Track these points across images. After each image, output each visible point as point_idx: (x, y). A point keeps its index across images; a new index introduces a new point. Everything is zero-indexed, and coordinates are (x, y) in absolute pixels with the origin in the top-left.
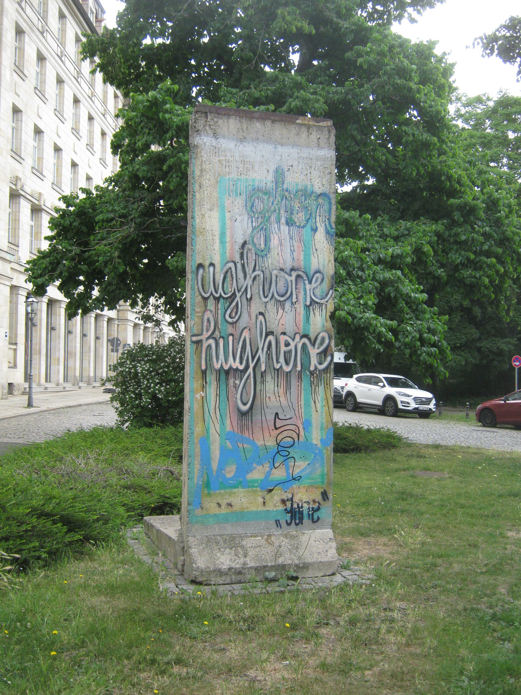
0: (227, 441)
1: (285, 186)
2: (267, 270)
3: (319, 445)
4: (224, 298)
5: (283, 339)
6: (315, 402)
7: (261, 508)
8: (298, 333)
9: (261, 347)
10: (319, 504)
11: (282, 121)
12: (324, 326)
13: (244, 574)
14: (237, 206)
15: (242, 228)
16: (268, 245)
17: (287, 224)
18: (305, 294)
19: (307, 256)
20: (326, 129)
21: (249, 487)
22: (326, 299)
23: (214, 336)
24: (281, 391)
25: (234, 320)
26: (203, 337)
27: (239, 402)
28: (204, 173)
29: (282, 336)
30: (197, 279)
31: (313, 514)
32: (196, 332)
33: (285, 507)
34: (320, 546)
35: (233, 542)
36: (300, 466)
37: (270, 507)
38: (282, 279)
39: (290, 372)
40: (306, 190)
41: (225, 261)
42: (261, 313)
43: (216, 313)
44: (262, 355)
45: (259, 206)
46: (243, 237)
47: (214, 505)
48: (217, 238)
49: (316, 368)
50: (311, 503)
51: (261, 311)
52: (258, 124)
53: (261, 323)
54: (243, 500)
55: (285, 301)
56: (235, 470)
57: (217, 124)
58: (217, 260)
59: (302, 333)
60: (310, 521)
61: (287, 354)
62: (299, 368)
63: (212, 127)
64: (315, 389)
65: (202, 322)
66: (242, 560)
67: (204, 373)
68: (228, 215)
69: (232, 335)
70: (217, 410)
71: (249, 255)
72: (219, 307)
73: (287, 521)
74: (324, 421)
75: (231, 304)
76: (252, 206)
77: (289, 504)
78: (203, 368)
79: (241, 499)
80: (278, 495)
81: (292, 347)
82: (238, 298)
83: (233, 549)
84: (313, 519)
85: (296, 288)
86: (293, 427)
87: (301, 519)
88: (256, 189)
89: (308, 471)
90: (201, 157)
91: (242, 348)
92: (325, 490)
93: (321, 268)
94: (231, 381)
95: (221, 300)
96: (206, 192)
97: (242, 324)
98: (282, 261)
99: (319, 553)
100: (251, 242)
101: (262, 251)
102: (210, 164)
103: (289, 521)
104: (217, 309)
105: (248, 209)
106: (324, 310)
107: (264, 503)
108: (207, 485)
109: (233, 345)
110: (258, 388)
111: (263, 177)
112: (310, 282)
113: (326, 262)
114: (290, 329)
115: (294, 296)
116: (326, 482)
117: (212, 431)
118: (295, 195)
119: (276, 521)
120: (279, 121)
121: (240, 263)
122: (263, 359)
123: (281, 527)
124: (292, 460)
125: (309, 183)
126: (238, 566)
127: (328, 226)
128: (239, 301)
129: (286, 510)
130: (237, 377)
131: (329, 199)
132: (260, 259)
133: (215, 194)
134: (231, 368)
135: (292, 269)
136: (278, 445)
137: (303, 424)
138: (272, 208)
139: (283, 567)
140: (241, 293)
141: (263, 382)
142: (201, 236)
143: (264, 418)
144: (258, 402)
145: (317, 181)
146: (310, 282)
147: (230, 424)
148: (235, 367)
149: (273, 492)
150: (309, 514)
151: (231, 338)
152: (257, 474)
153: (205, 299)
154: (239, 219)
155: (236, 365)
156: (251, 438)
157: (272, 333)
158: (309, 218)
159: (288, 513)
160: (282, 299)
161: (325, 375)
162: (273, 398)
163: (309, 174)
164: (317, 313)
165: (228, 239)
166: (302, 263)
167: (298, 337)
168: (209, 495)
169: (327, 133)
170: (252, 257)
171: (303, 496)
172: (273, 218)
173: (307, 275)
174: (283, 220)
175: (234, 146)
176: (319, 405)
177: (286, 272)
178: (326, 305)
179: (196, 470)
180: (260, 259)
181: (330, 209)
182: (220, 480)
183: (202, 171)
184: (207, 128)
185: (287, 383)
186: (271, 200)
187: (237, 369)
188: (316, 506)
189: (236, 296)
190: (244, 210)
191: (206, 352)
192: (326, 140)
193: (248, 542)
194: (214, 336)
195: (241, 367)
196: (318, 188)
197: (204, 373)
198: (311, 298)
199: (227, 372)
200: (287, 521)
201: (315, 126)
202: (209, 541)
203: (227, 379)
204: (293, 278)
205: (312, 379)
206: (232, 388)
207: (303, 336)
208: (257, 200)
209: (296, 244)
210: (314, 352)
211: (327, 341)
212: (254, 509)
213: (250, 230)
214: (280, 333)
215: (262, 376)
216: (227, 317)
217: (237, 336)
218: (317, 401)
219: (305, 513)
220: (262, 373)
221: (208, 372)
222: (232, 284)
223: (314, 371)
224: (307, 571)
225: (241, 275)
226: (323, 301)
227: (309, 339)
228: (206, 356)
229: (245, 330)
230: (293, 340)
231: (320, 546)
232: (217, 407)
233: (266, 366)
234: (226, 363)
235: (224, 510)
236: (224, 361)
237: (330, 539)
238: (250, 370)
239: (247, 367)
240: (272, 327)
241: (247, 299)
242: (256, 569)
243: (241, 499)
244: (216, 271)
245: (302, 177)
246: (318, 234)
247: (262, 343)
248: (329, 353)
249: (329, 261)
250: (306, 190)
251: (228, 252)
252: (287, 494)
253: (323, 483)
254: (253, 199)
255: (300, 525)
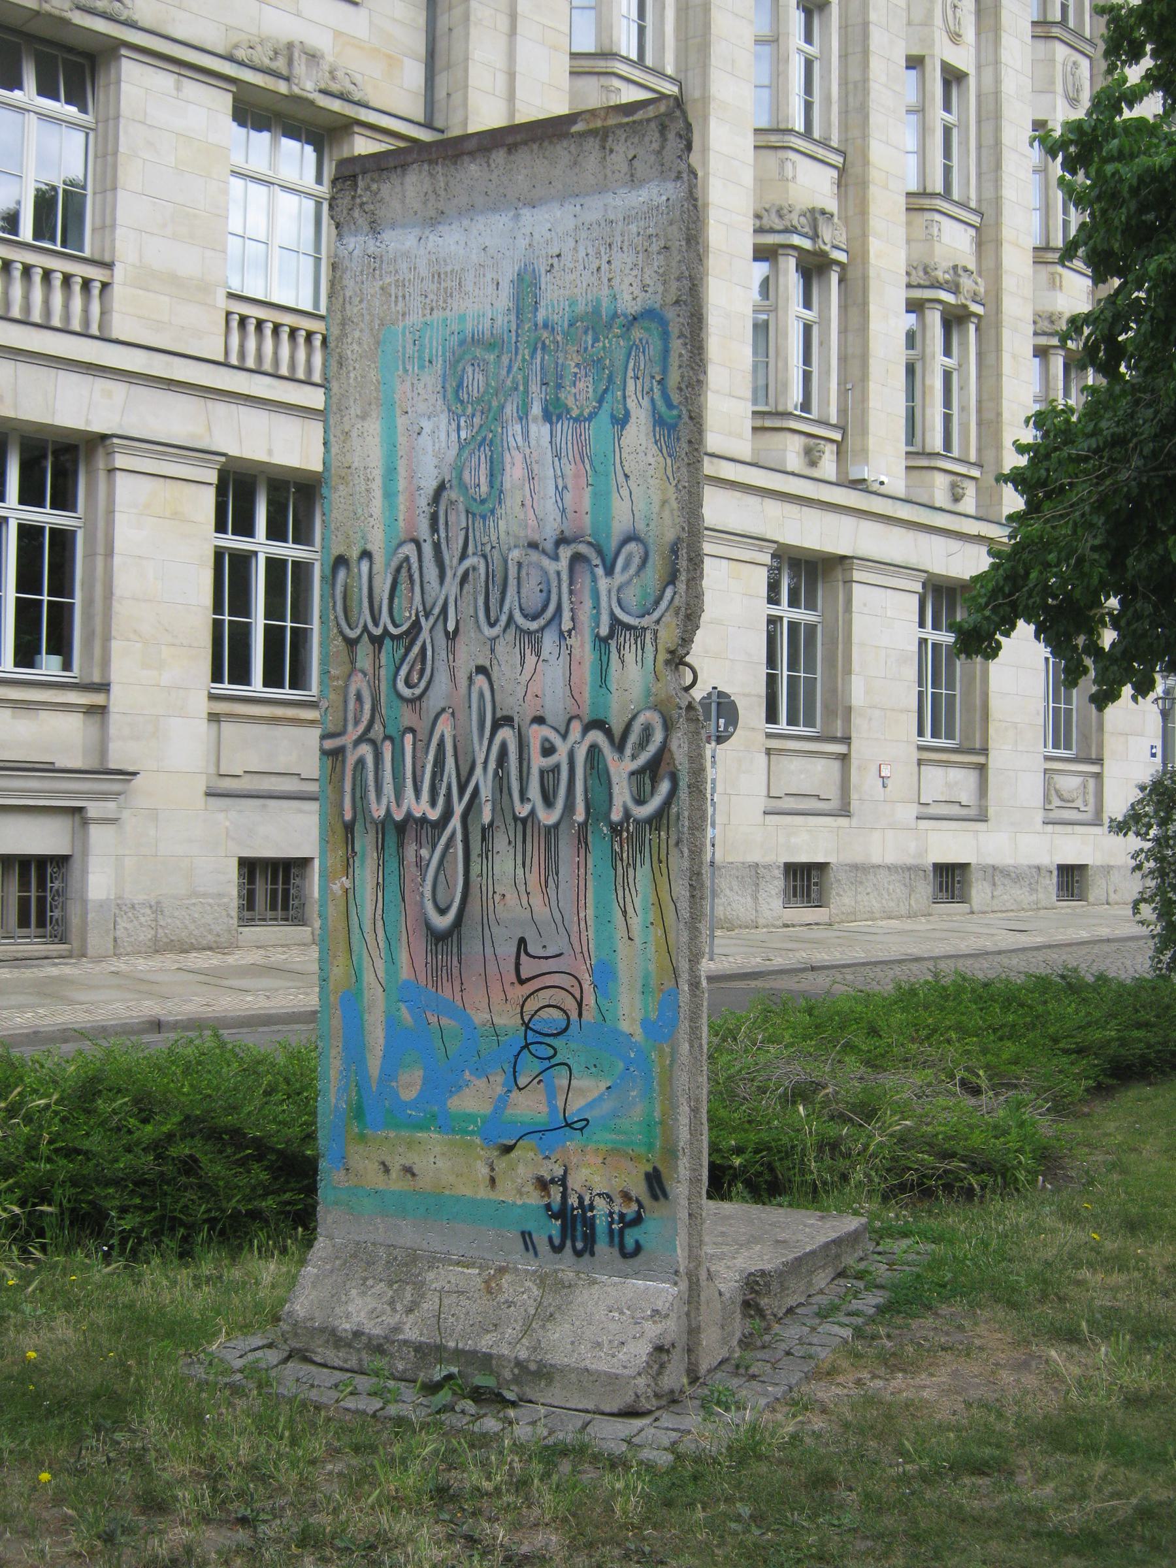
0: (402, 1006)
1: (541, 315)
2: (496, 553)
3: (639, 1036)
4: (393, 638)
5: (537, 734)
6: (625, 913)
7: (483, 1193)
8: (577, 717)
9: (480, 759)
10: (641, 1206)
11: (533, 140)
12: (648, 693)
13: (392, 1356)
14: (422, 395)
15: (434, 446)
16: (497, 485)
17: (547, 416)
18: (597, 606)
19: (601, 498)
20: (653, 125)
21: (453, 1131)
22: (656, 615)
23: (372, 735)
24: (533, 878)
25: (418, 691)
26: (348, 740)
27: (429, 906)
28: (348, 329)
29: (535, 727)
30: (333, 596)
31: (621, 1230)
32: (331, 728)
33: (546, 1200)
34: (613, 1327)
35: (405, 1271)
36: (586, 1092)
37: (506, 1192)
38: (533, 571)
39: (556, 826)
40: (596, 311)
41: (395, 542)
42: (481, 670)
43: (376, 676)
44: (483, 779)
45: (475, 381)
46: (436, 472)
47: (373, 1167)
48: (377, 487)
49: (627, 815)
50: (618, 1200)
51: (480, 662)
52: (473, 167)
53: (481, 695)
54: (440, 1164)
55: (542, 629)
56: (420, 1082)
57: (378, 197)
58: (377, 543)
59: (587, 715)
60: (616, 1251)
61: (549, 776)
62: (580, 816)
63: (366, 208)
64: (625, 875)
65: (345, 702)
66: (391, 1320)
67: (349, 828)
68: (401, 421)
69: (412, 730)
70: (379, 923)
71: (452, 518)
72: (383, 662)
73: (550, 1239)
74: (652, 967)
75: (408, 650)
76: (460, 385)
77: (556, 1192)
78: (348, 816)
79: (436, 1160)
80: (527, 1165)
81: (561, 756)
82: (425, 635)
83: (395, 1286)
84: (622, 1247)
85: (571, 592)
86: (565, 981)
87: (590, 1240)
88: (469, 339)
89: (607, 1107)
90: (343, 288)
91: (435, 765)
92: (655, 1169)
93: (641, 527)
94: (410, 850)
95: (387, 642)
96: (352, 375)
97: (435, 700)
98: (532, 522)
99: (599, 1345)
100: (454, 482)
101: (483, 502)
102: (361, 301)
103: (557, 1242)
104: (377, 667)
105: (450, 395)
106: (649, 648)
107: (493, 1180)
108: (358, 1112)
109: (414, 757)
110: (475, 868)
111: (485, 304)
112: (609, 572)
113: (656, 508)
114: (555, 705)
115: (566, 615)
116: (658, 1144)
117: (368, 977)
118: (566, 334)
119: (523, 1233)
120: (525, 143)
121: (429, 541)
122: (486, 793)
123: (536, 1254)
124: (564, 1071)
125: (606, 291)
126: (377, 1331)
127: (660, 403)
128: (428, 641)
129: (548, 1207)
130: (424, 841)
131: (663, 322)
132: (479, 523)
133: (373, 375)
134: (409, 815)
135: (562, 540)
136: (527, 1026)
137: (591, 971)
138: (509, 383)
139: (485, 1361)
140: (432, 619)
141: (487, 853)
142: (341, 487)
143: (489, 951)
144: (474, 907)
145: (627, 281)
146: (609, 572)
147: (410, 959)
148: (418, 815)
149: (513, 1155)
150: (611, 1231)
151: (409, 738)
152: (473, 1100)
153: (351, 643)
154: (427, 426)
155: (422, 808)
156: (459, 1003)
157: (508, 720)
158: (606, 391)
159: (555, 1216)
160: (534, 626)
161: (654, 836)
162: (512, 898)
163: (604, 267)
164: (630, 657)
165: (402, 484)
166: (587, 520)
167: (576, 728)
168: (362, 1138)
169: (657, 135)
170: (458, 520)
171: (595, 1178)
172: (510, 410)
173: (600, 552)
174: (536, 410)
175: (414, 241)
176: (636, 922)
177: (544, 552)
178: (656, 632)
179: (332, 1073)
180: (479, 523)
181: (666, 352)
182: (387, 1103)
183: (343, 324)
184: (356, 213)
185: (548, 858)
186: (505, 360)
187: (424, 820)
188: (631, 1210)
189: (421, 628)
190: (440, 402)
191: (354, 779)
192: (653, 157)
193: (437, 1279)
194: (372, 735)
195: (434, 815)
196: (629, 304)
197: (349, 828)
198: (612, 615)
199: (401, 828)
200: (550, 1239)
201: (620, 126)
202: (354, 1256)
203: (401, 845)
204: (563, 564)
205: (617, 847)
206: (413, 869)
207: (586, 729)
208: (469, 369)
209: (569, 470)
210: (621, 769)
211: (658, 736)
212: (469, 1193)
213: (454, 452)
214: (529, 719)
215: (483, 839)
216: (401, 685)
217: (422, 735)
218: (630, 910)
219: (601, 1224)
220: (483, 829)
221: (358, 827)
222: (412, 599)
223: (621, 824)
224: (549, 1384)
225: (431, 572)
226: (646, 622)
227: (608, 733)
228: (353, 789)
229: (444, 717)
230: (564, 736)
231: (613, 1327)
232: (378, 917)
233: (493, 810)
234: (398, 805)
235: (397, 1183)
236: (393, 799)
237: (656, 1312)
238: (455, 822)
239: (447, 814)
240: (510, 704)
241: (447, 633)
242: (419, 1348)
243: (436, 1160)
244: (375, 571)
245: (587, 277)
246: (631, 430)
247: (485, 749)
248: (664, 769)
249: (664, 502)
250: (596, 311)
251: (401, 518)
252: (549, 1164)
253: (650, 1146)
254: (460, 368)
255: (587, 1256)
